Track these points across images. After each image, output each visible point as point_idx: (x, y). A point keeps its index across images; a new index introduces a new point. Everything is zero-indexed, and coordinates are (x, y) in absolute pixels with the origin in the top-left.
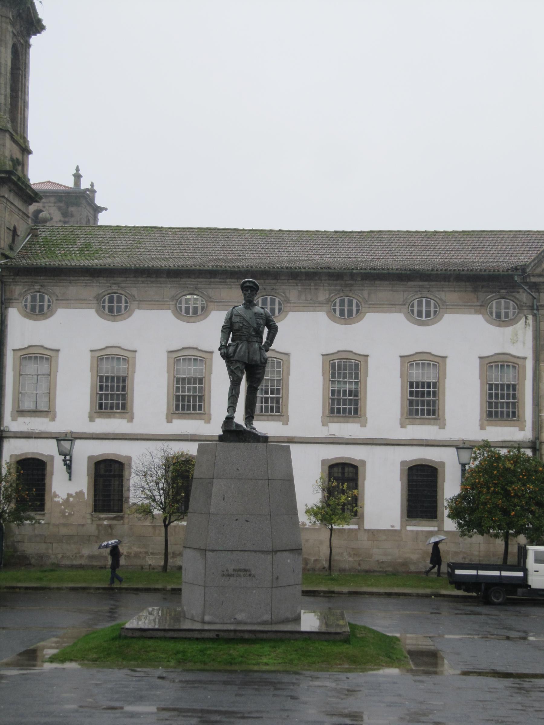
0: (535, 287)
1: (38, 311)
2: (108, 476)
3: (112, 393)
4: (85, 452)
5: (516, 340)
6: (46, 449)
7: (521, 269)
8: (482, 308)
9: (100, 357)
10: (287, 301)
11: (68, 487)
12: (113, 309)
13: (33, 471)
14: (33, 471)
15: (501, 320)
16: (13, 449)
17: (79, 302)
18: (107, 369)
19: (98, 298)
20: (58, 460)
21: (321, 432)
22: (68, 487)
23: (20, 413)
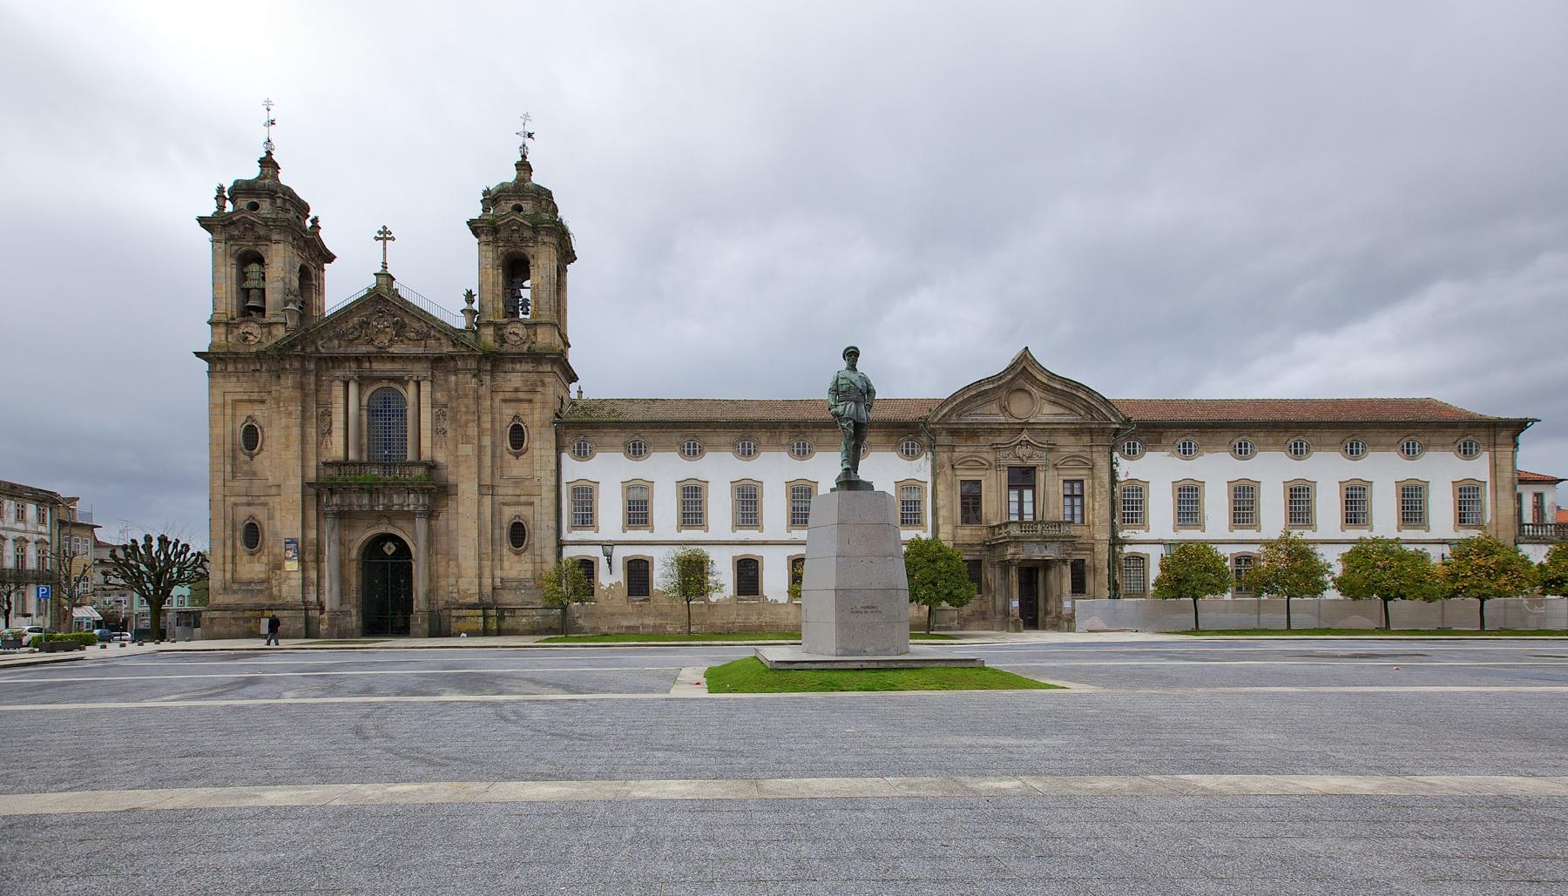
0: (932, 431)
1: (582, 454)
2: (638, 573)
3: (638, 513)
4: (620, 554)
5: (920, 469)
6: (594, 552)
7: (925, 421)
8: (896, 447)
9: (629, 486)
10: (760, 444)
11: (610, 578)
12: (636, 451)
13: (588, 565)
14: (588, 565)
15: (910, 455)
16: (569, 552)
17: (611, 447)
18: (636, 495)
19: (625, 444)
20: (603, 561)
21: (787, 537)
22: (610, 578)
23: (573, 527)
